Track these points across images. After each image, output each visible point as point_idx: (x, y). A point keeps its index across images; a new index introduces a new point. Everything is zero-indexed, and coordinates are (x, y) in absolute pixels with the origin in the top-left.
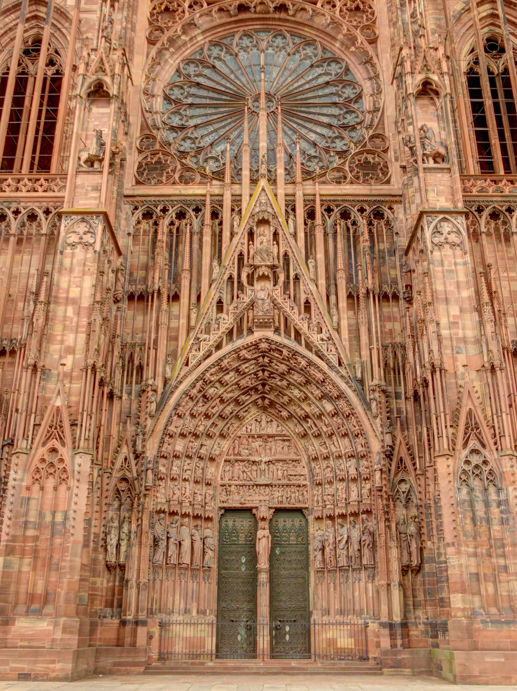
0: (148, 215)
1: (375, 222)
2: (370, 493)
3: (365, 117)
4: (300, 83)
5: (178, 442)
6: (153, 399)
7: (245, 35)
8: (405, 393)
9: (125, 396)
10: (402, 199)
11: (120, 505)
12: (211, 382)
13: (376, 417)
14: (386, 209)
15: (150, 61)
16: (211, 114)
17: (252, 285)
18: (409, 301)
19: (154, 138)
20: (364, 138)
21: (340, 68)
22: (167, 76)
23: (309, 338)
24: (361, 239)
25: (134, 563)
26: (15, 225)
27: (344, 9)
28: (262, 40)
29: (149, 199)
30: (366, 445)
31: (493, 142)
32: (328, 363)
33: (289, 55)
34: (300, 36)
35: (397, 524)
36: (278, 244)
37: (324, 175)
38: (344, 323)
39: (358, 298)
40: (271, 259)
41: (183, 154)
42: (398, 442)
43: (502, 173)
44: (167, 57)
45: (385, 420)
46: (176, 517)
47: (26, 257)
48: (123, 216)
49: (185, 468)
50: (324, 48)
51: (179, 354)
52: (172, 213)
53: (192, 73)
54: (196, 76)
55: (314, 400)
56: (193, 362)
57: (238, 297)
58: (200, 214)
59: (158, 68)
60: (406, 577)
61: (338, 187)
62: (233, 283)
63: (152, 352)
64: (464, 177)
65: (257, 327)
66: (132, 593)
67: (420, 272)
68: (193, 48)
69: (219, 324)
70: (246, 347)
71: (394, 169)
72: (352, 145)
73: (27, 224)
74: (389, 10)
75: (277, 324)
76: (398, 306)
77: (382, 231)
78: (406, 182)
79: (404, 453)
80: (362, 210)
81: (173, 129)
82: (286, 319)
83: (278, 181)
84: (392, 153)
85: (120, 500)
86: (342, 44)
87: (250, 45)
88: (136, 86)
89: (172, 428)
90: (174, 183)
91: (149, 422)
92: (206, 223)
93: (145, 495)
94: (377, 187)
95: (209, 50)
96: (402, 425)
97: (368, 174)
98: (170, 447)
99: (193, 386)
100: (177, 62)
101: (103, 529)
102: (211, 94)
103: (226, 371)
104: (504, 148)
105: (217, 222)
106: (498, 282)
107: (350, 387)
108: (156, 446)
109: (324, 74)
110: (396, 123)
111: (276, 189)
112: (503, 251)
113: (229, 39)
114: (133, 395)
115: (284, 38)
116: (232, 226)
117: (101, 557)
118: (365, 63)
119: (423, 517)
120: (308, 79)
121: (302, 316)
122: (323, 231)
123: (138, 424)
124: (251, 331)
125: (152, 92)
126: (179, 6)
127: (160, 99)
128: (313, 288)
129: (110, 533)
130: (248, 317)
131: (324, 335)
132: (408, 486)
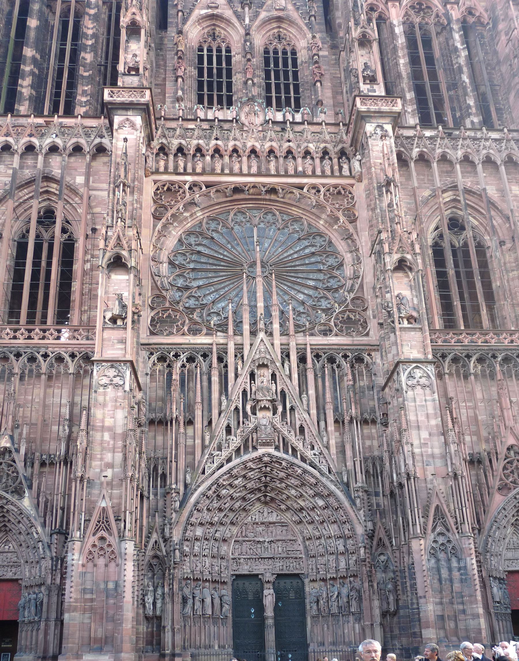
0: (162, 359)
1: (356, 366)
2: (356, 563)
3: (346, 281)
4: (289, 253)
5: (198, 529)
6: (177, 499)
7: (239, 212)
8: (383, 492)
9: (152, 497)
10: (379, 348)
11: (154, 575)
12: (223, 485)
13: (360, 510)
14: (366, 355)
15: (156, 234)
16: (211, 277)
17: (255, 414)
18: (386, 425)
19: (164, 298)
20: (346, 300)
21: (325, 241)
22: (171, 245)
23: (304, 453)
24: (345, 378)
25: (168, 615)
26: (44, 366)
27: (328, 193)
28: (255, 217)
29: (162, 346)
30: (353, 529)
31: (455, 303)
32: (320, 471)
33: (279, 229)
34: (288, 214)
35: (378, 584)
36: (276, 383)
37: (313, 328)
38: (332, 442)
39: (343, 422)
40: (271, 395)
41: (191, 310)
42: (377, 528)
43: (462, 328)
44: (170, 229)
45: (367, 512)
46: (201, 583)
47: (57, 391)
48: (141, 360)
49: (204, 547)
50: (309, 224)
51: (196, 465)
52: (183, 357)
53: (193, 243)
54: (196, 245)
55: (308, 498)
56: (208, 472)
57: (243, 423)
58: (208, 359)
59: (162, 239)
60: (385, 620)
61: (325, 338)
62: (238, 412)
63: (174, 464)
64: (433, 331)
65: (261, 445)
66: (168, 637)
67: (395, 404)
68: (193, 222)
69: (229, 444)
70: (253, 460)
71: (373, 325)
72: (336, 305)
73: (56, 365)
74: (368, 196)
75: (277, 443)
76: (376, 428)
77: (363, 371)
78: (383, 336)
79: (382, 534)
80: (345, 357)
81: (179, 289)
82: (284, 439)
83: (274, 333)
84: (371, 312)
85: (153, 571)
86: (326, 222)
87: (244, 220)
88: (146, 255)
89: (193, 520)
90: (183, 334)
91: (174, 515)
92: (213, 366)
93: (174, 568)
94: (358, 339)
95: (207, 223)
96: (380, 515)
97: (350, 328)
98: (192, 533)
99: (209, 489)
100: (180, 233)
101: (141, 592)
102: (211, 261)
103: (236, 477)
104: (463, 308)
105: (222, 365)
106: (458, 410)
107: (338, 488)
108: (181, 532)
109: (310, 246)
110: (374, 288)
111: (273, 339)
112: (462, 387)
113: (225, 215)
114: (159, 496)
115: (274, 215)
116: (236, 369)
117: (141, 611)
118: (347, 239)
119: (398, 578)
120: (296, 250)
121: (297, 437)
122: (313, 373)
123: (165, 516)
124: (255, 448)
125: (159, 257)
126: (180, 187)
127: (165, 265)
128: (306, 416)
129: (147, 595)
130: (252, 438)
131: (316, 451)
132: (386, 558)
